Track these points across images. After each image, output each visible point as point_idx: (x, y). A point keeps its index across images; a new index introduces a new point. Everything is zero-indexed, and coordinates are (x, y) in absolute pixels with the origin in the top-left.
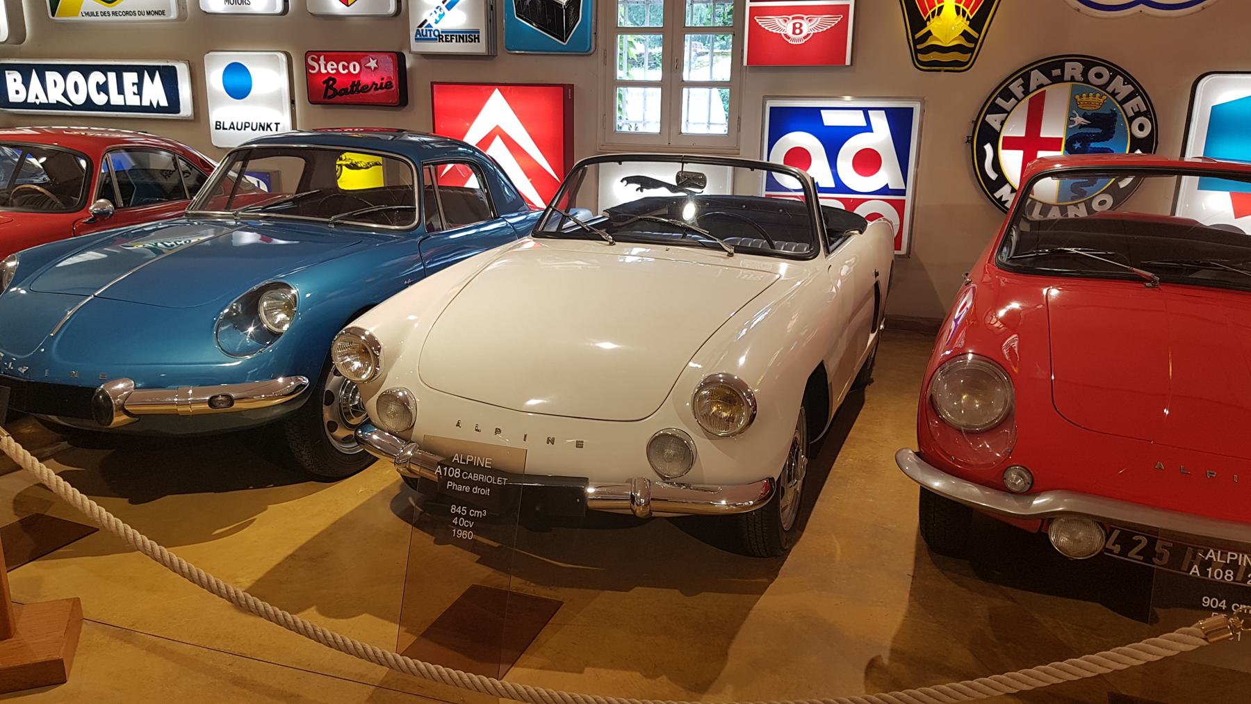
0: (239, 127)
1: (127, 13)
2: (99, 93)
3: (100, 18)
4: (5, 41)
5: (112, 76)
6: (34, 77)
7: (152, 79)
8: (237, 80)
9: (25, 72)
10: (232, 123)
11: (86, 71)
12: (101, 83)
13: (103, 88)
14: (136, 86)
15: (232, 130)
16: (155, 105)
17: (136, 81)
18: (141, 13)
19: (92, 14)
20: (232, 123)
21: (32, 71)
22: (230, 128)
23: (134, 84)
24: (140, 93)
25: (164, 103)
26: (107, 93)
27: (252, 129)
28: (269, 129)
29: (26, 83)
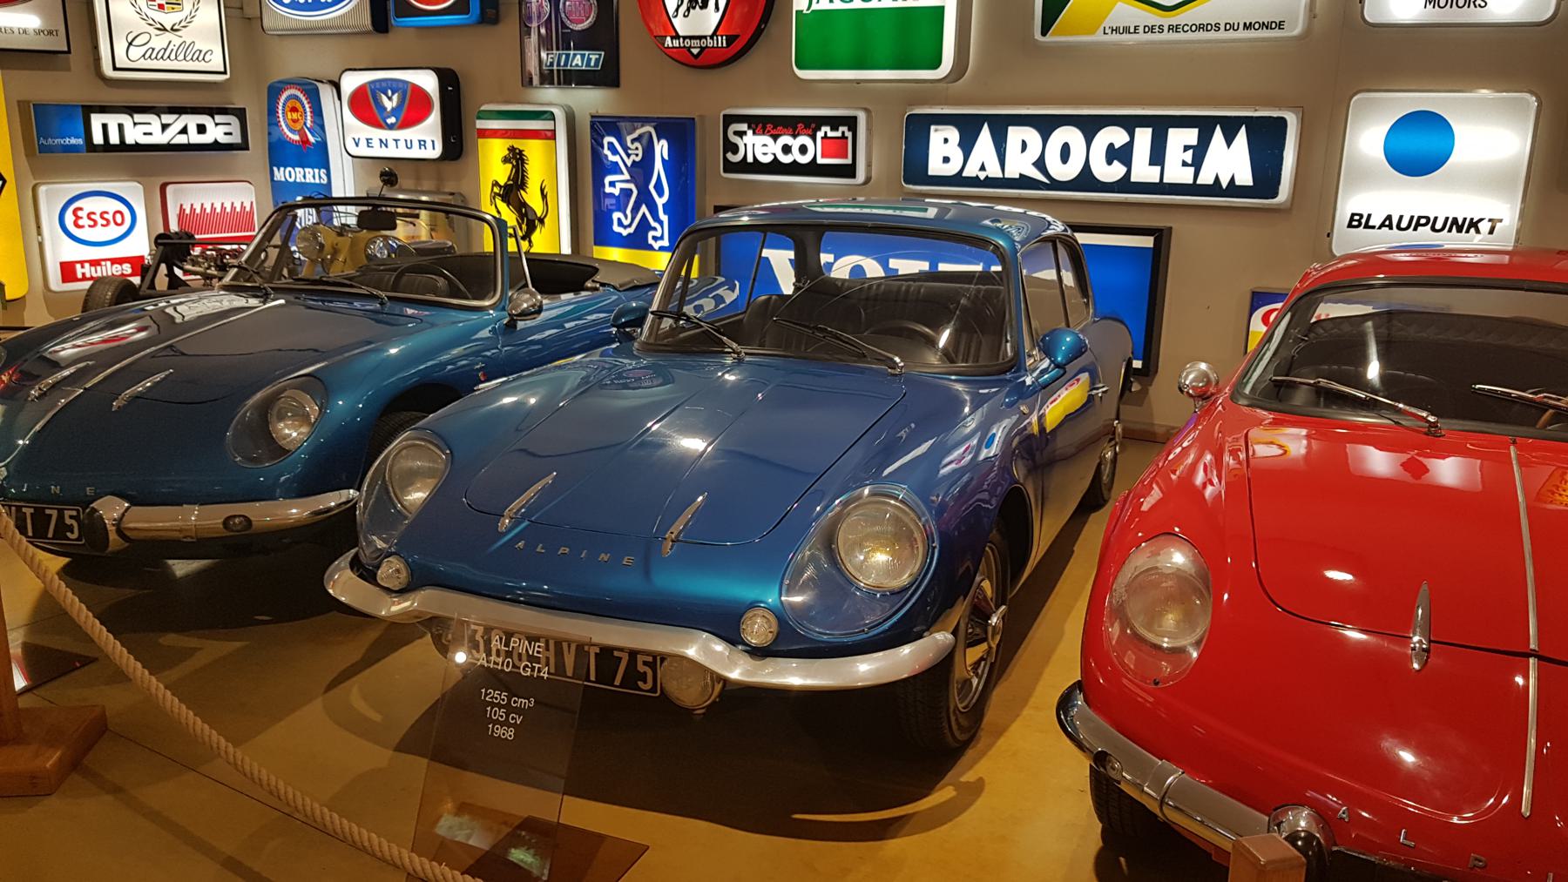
0: (1404, 225)
1: (1201, 27)
2: (1109, 162)
3: (1141, 37)
4: (944, 78)
5: (1144, 136)
6: (985, 135)
7: (1229, 140)
8: (1419, 143)
9: (968, 130)
10: (1389, 218)
11: (1089, 127)
12: (1117, 146)
13: (1120, 155)
14: (1190, 152)
15: (1385, 229)
16: (1224, 185)
17: (1194, 142)
18: (1232, 27)
19: (1126, 30)
20: (1389, 218)
22: (1382, 225)
23: (1186, 148)
24: (1197, 163)
25: (1245, 178)
26: (1127, 162)
27: (1433, 229)
28: (1472, 230)
29: (967, 145)
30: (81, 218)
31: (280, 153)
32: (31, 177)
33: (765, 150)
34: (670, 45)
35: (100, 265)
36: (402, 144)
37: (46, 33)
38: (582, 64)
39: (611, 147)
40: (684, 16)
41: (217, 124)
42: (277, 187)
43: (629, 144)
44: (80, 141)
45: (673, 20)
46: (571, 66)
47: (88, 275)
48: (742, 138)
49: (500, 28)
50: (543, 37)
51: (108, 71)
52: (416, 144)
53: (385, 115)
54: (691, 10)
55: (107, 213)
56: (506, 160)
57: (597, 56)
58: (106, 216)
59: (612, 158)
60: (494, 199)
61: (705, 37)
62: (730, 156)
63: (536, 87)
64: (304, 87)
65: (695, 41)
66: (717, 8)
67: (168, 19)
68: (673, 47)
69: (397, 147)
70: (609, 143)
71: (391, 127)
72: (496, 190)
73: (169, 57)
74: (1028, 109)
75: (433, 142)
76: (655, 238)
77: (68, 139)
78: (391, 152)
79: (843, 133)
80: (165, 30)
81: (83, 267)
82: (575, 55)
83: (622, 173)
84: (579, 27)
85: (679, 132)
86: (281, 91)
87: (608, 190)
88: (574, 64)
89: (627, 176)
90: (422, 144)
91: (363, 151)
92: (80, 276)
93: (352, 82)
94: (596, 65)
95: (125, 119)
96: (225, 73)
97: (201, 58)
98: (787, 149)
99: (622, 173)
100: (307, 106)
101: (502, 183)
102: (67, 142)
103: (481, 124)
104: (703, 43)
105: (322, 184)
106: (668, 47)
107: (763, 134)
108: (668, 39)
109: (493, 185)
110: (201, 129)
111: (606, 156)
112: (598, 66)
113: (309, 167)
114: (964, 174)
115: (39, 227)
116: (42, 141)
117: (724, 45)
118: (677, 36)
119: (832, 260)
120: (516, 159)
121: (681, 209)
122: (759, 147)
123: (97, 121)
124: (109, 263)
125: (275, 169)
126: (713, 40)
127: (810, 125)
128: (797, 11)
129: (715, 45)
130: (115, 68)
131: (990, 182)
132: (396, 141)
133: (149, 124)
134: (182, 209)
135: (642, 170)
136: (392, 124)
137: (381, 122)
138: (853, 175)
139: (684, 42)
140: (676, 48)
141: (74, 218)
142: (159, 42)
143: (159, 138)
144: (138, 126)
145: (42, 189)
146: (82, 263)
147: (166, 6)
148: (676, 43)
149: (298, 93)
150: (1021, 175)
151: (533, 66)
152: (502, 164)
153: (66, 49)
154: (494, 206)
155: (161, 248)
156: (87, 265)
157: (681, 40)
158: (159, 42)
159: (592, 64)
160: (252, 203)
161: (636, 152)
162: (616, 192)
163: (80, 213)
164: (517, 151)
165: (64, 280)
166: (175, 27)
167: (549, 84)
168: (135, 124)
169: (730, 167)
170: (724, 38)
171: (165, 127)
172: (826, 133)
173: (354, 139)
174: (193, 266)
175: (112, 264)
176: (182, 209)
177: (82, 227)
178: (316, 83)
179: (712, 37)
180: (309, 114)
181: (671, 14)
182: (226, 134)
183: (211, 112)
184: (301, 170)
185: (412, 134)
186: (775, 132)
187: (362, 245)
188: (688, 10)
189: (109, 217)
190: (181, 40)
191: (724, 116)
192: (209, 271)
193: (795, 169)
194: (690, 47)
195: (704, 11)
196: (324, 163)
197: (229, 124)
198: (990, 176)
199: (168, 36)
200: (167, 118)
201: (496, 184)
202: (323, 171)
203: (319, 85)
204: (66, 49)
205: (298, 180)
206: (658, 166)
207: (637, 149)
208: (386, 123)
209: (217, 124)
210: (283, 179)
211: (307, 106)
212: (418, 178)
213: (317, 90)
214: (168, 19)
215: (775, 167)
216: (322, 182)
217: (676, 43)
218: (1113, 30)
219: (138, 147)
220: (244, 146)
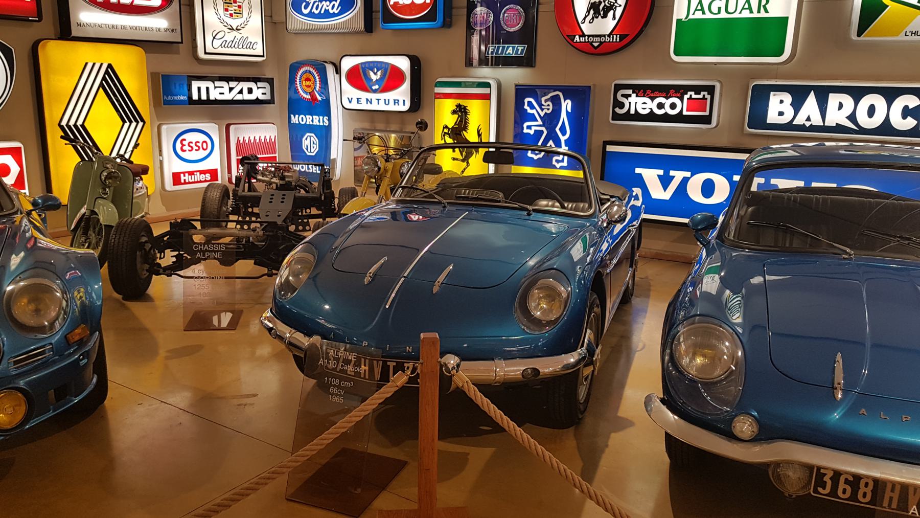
2: (904, 117)
11: (891, 95)
12: (911, 107)
21: (810, 92)
29: (797, 105)
30: (185, 145)
31: (295, 106)
32: (156, 119)
33: (644, 106)
34: (578, 41)
35: (194, 174)
36: (382, 102)
37: (170, 30)
38: (513, 52)
39: (530, 104)
40: (590, 22)
41: (258, 88)
42: (292, 127)
43: (543, 102)
44: (185, 98)
45: (582, 25)
46: (505, 54)
47: (187, 181)
48: (628, 99)
49: (451, 30)
50: (483, 36)
51: (201, 54)
52: (392, 102)
53: (371, 84)
54: (595, 19)
55: (198, 142)
56: (454, 112)
57: (523, 48)
58: (198, 144)
59: (529, 111)
60: (444, 135)
61: (604, 36)
62: (617, 110)
63: (475, 67)
64: (316, 67)
65: (597, 38)
66: (614, 18)
67: (235, 23)
68: (580, 42)
69: (378, 104)
70: (528, 102)
71: (375, 91)
72: (446, 131)
73: (234, 46)
74: (841, 82)
75: (404, 101)
76: (558, 161)
77: (179, 97)
78: (374, 107)
79: (704, 96)
80: (233, 29)
81: (184, 176)
82: (508, 47)
83: (537, 121)
84: (513, 30)
85: (580, 95)
86: (299, 68)
87: (525, 131)
88: (507, 53)
89: (540, 122)
90: (396, 102)
91: (354, 105)
92: (183, 181)
93: (348, 63)
94: (522, 53)
95: (210, 84)
96: (263, 56)
97: (251, 47)
98: (660, 106)
99: (537, 120)
100: (317, 78)
101: (450, 126)
102: (179, 99)
103: (438, 90)
104: (603, 39)
105: (325, 126)
106: (576, 42)
107: (644, 96)
108: (577, 37)
109: (444, 128)
110: (250, 91)
111: (526, 110)
112: (503, 54)
113: (309, 115)
114: (794, 123)
115: (160, 151)
116: (165, 98)
117: (618, 40)
118: (583, 35)
119: (689, 176)
120: (461, 111)
121: (578, 141)
122: (640, 104)
123: (195, 85)
124: (198, 173)
125: (292, 116)
126: (610, 37)
127: (679, 91)
128: (677, 20)
129: (611, 41)
130: (206, 53)
131: (813, 128)
132: (378, 100)
133: (223, 87)
134: (238, 140)
135: (551, 120)
136: (375, 89)
137: (369, 89)
138: (710, 123)
139: (588, 39)
140: (582, 42)
142: (230, 37)
143: (228, 96)
144: (217, 89)
145: (164, 128)
146: (184, 173)
147: (234, 14)
148: (582, 39)
149: (312, 70)
150: (837, 124)
151: (475, 54)
152: (451, 115)
153: (180, 41)
154: (443, 140)
155: (246, 165)
156: (187, 175)
157: (587, 37)
158: (230, 37)
159: (519, 53)
160: (275, 136)
161: (548, 107)
162: (532, 132)
163: (184, 143)
164: (463, 107)
166: (239, 28)
167: (485, 65)
168: (215, 87)
169: (616, 117)
170: (618, 36)
171: (231, 89)
172: (691, 96)
173: (348, 98)
174: (263, 177)
175: (200, 174)
176: (238, 140)
177: (185, 151)
178: (324, 63)
179: (609, 36)
180: (318, 82)
181: (580, 22)
182: (263, 94)
183: (256, 80)
184: (310, 117)
185: (391, 95)
186: (652, 95)
187: (399, 167)
188: (593, 18)
189: (200, 145)
190: (241, 36)
191: (615, 85)
192: (272, 180)
193: (666, 118)
194: (593, 42)
195: (604, 19)
196: (327, 111)
197: (265, 88)
198: (813, 124)
199: (234, 33)
200: (232, 84)
201: (446, 127)
202: (326, 118)
203: (326, 64)
204: (180, 41)
205: (308, 123)
206: (564, 116)
207: (549, 105)
208: (372, 89)
209: (258, 88)
210: (297, 122)
211: (317, 78)
212: (388, 122)
213: (325, 68)
214: (235, 23)
215: (651, 117)
216: (325, 124)
217: (582, 39)
218: (912, 33)
219: (216, 102)
220: (271, 101)
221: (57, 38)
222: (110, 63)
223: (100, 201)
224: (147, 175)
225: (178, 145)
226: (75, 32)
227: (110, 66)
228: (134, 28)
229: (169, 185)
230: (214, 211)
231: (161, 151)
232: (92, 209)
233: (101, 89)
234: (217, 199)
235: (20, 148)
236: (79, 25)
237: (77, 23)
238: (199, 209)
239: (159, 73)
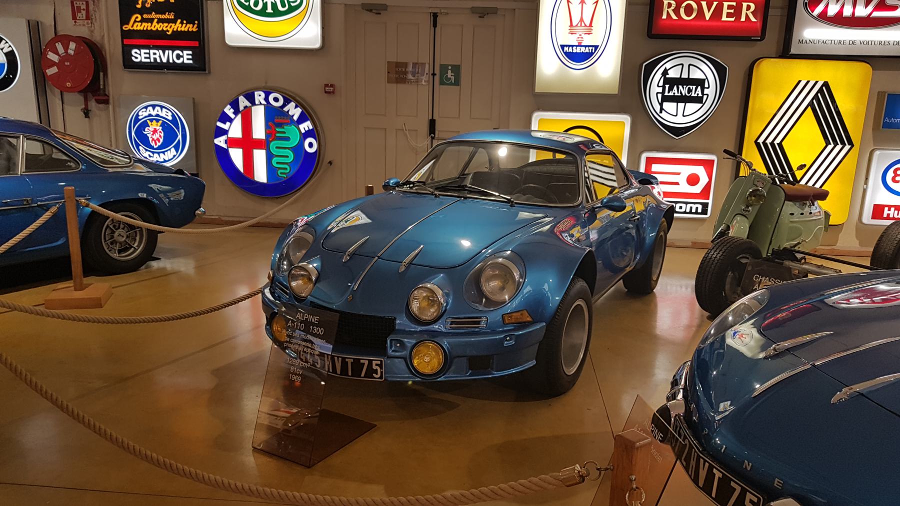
47: (891, 216)
81: (889, 210)
92: (885, 215)
115: (867, 179)
141: (894, 175)
146: (890, 207)
165: (874, 217)
221: (778, 56)
222: (826, 81)
223: (739, 218)
224: (825, 201)
225: (890, 174)
226: (793, 51)
227: (826, 84)
228: (865, 43)
229: (867, 218)
230: (888, 253)
231: (867, 179)
232: (728, 224)
233: (809, 108)
234: (897, 239)
235: (714, 161)
236: (800, 42)
237: (799, 40)
238: (872, 249)
239: (886, 92)
